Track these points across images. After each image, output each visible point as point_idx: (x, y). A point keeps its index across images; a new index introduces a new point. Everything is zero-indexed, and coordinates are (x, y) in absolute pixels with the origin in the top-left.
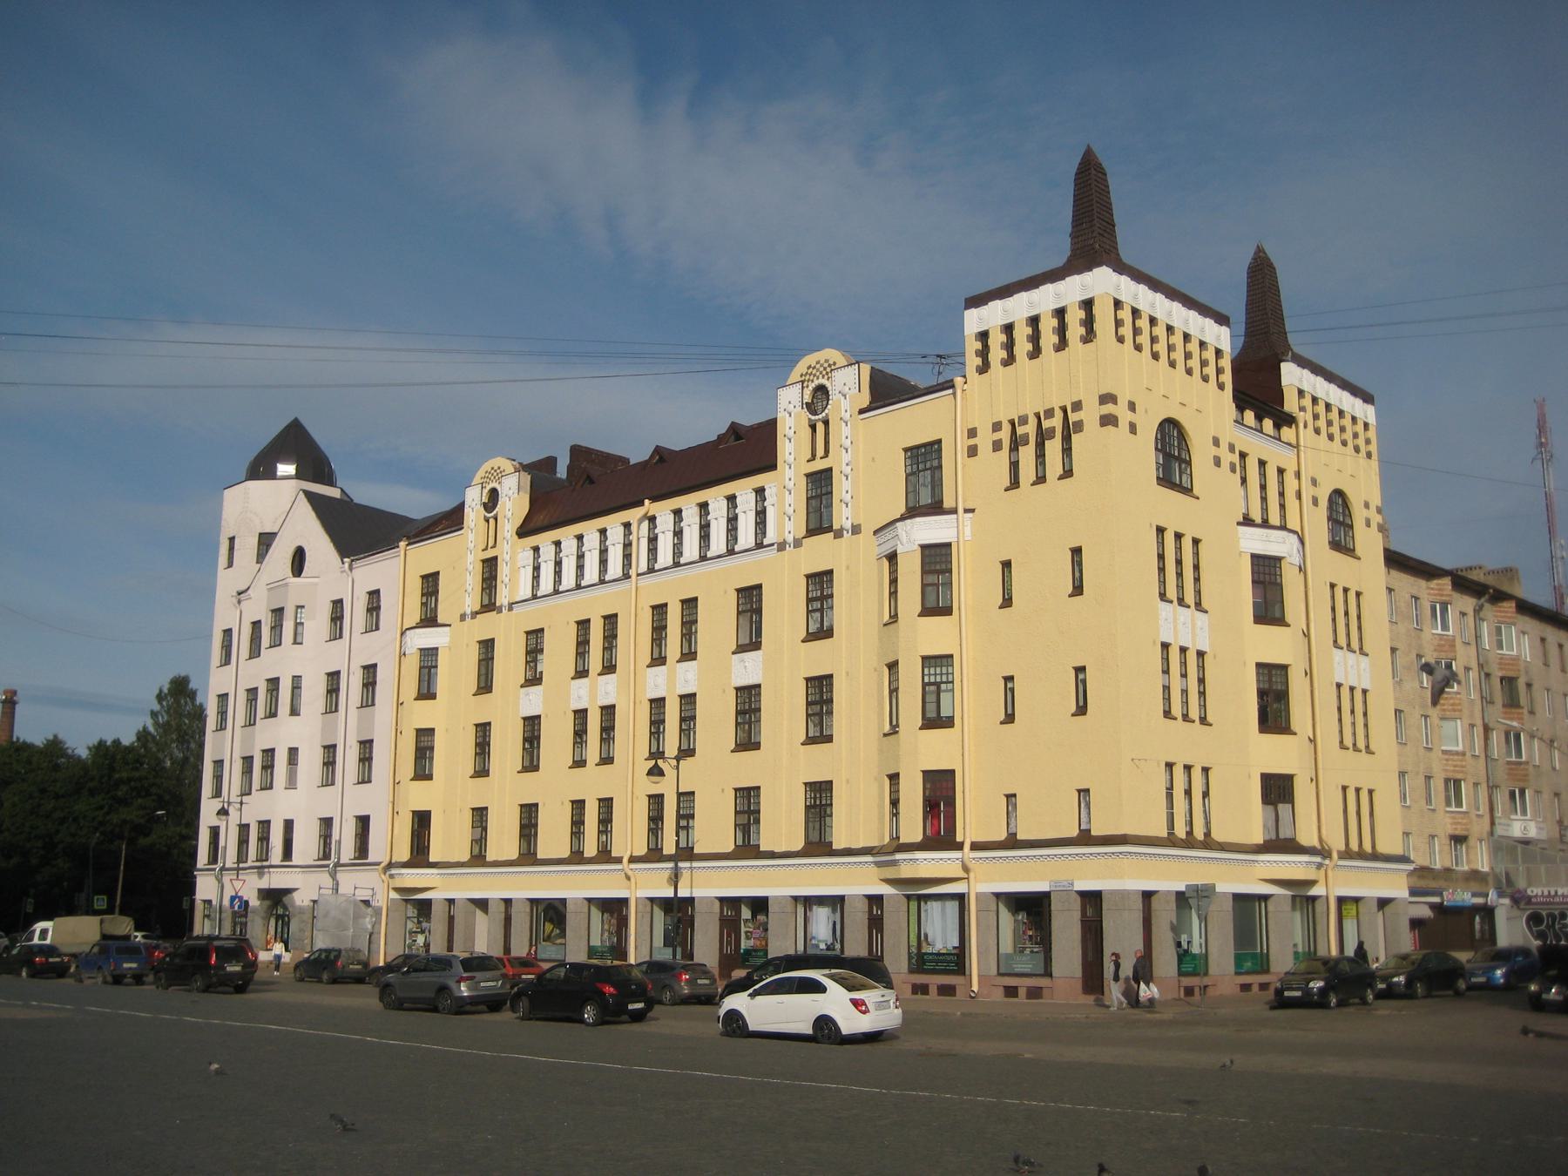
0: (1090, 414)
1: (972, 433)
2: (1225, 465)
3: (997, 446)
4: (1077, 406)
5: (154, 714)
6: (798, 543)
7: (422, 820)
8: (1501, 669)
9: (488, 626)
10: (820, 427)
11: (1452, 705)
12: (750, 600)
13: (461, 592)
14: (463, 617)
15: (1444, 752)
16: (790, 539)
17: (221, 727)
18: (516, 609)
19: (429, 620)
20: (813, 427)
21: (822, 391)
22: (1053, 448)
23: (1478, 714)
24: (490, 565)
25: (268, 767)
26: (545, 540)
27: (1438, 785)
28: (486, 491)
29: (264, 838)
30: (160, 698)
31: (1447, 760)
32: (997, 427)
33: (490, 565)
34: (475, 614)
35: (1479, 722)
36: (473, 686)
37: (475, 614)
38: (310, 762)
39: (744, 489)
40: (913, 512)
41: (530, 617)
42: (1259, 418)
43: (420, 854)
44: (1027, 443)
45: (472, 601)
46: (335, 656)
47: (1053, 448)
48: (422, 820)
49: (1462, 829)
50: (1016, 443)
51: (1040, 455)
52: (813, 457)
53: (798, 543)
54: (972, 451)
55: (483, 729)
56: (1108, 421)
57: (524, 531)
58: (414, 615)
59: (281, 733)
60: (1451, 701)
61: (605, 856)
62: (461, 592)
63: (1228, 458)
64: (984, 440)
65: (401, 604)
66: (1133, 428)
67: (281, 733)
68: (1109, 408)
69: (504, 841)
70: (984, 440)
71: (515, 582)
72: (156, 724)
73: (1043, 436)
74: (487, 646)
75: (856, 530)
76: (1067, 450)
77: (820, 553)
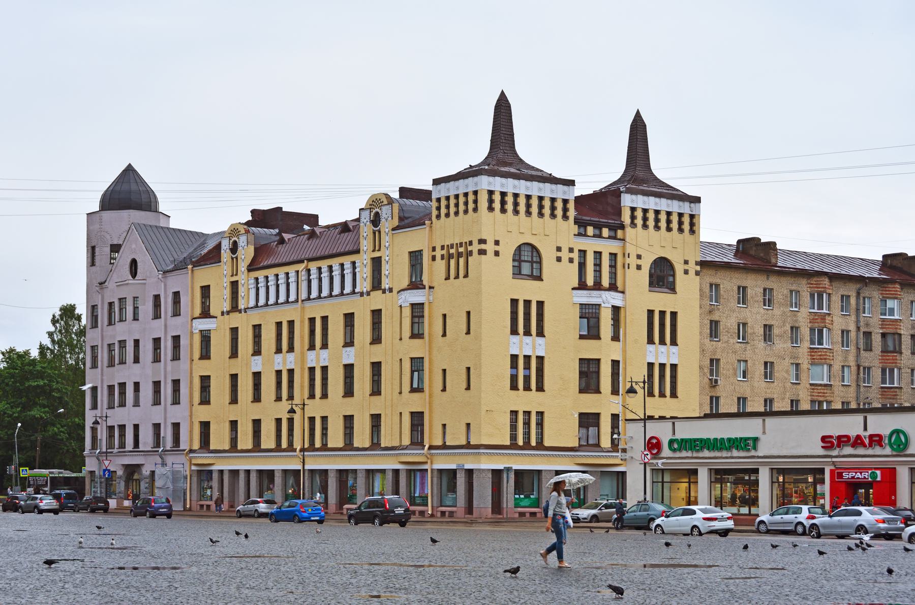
0: (475, 248)
1: (434, 249)
3: (442, 257)
4: (471, 243)
5: (51, 334)
6: (368, 294)
7: (205, 426)
8: (882, 328)
9: (236, 320)
10: (377, 233)
11: (820, 355)
12: (349, 318)
13: (220, 301)
14: (223, 314)
15: (811, 385)
17: (94, 366)
18: (249, 312)
19: (206, 314)
20: (374, 233)
21: (377, 214)
22: (462, 261)
24: (235, 285)
25: (123, 393)
26: (261, 274)
28: (231, 241)
29: (122, 435)
30: (54, 321)
31: (813, 389)
32: (443, 247)
33: (235, 285)
34: (228, 313)
35: (852, 363)
36: (228, 354)
37: (228, 313)
38: (147, 392)
39: (347, 261)
41: (255, 318)
42: (598, 227)
45: (227, 306)
46: (157, 329)
47: (462, 261)
50: (450, 256)
52: (374, 251)
53: (368, 294)
54: (434, 258)
55: (234, 378)
56: (482, 252)
57: (251, 268)
58: (198, 311)
59: (128, 374)
60: (820, 354)
61: (324, 447)
62: (220, 301)
63: (565, 255)
64: (438, 253)
65: (191, 303)
66: (497, 253)
67: (128, 374)
68: (483, 246)
69: (245, 441)
70: (438, 253)
71: (246, 299)
72: (53, 341)
73: (460, 255)
74: (234, 331)
75: (391, 290)
77: (377, 300)
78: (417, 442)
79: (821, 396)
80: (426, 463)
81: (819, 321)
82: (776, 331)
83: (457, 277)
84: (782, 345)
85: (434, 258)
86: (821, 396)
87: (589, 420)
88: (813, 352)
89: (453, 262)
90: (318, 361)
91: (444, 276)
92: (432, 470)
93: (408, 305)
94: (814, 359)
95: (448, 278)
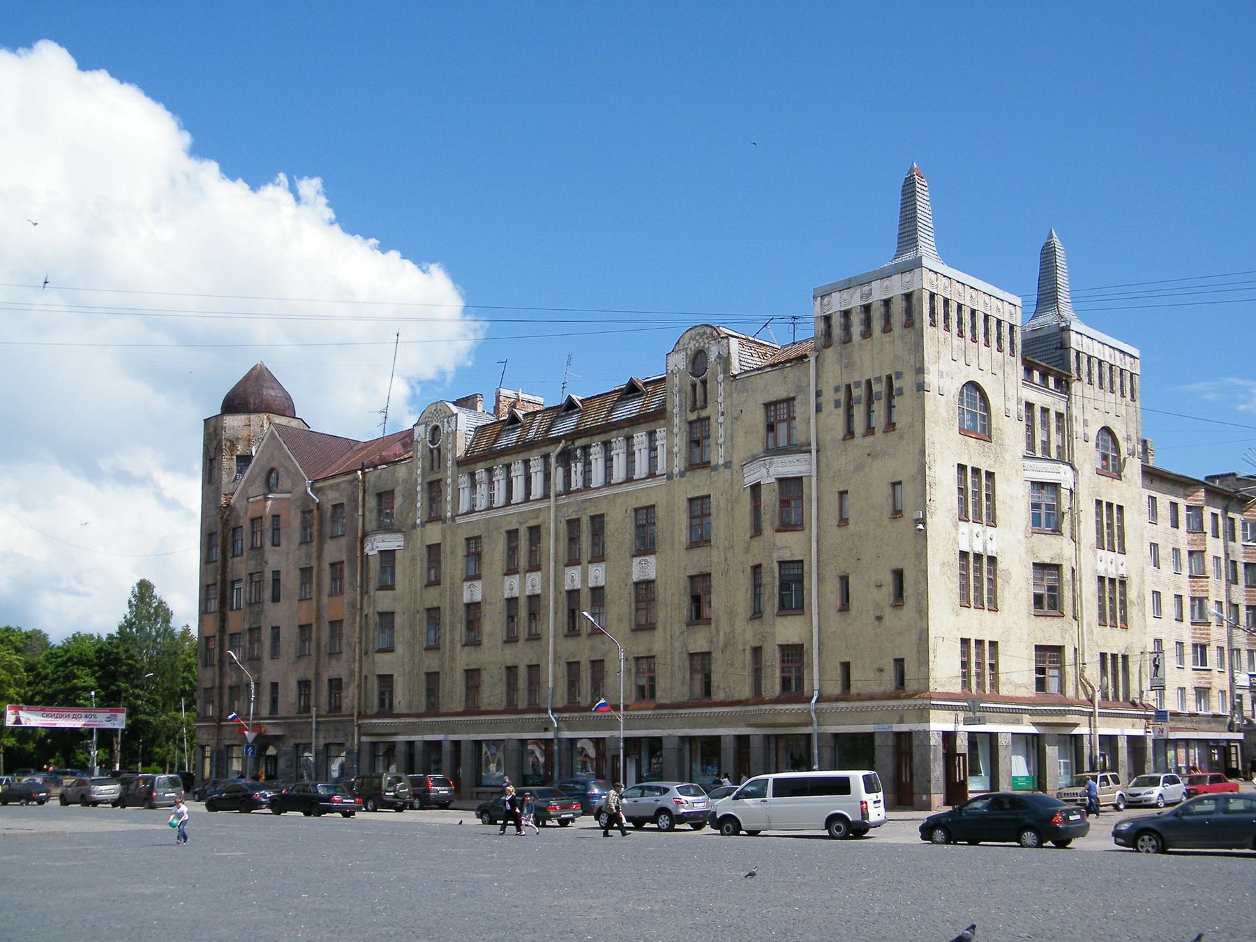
2: (1014, 414)
3: (837, 404)
6: (682, 474)
8: (1245, 557)
11: (1201, 586)
16: (676, 470)
22: (879, 407)
23: (1223, 593)
27: (1188, 650)
31: (1195, 629)
32: (837, 389)
40: (773, 451)
43: (386, 708)
44: (860, 403)
47: (879, 407)
48: (386, 681)
49: (1206, 683)
51: (869, 412)
75: (728, 465)
76: (890, 407)
78: (792, 689)
79: (1203, 638)
80: (810, 724)
81: (1197, 542)
82: (1162, 552)
83: (870, 430)
84: (1167, 568)
85: (819, 409)
86: (1203, 638)
87: (1049, 655)
88: (1193, 582)
89: (859, 412)
90: (584, 579)
91: (840, 431)
92: (820, 735)
93: (773, 480)
94: (1194, 591)
95: (850, 433)
